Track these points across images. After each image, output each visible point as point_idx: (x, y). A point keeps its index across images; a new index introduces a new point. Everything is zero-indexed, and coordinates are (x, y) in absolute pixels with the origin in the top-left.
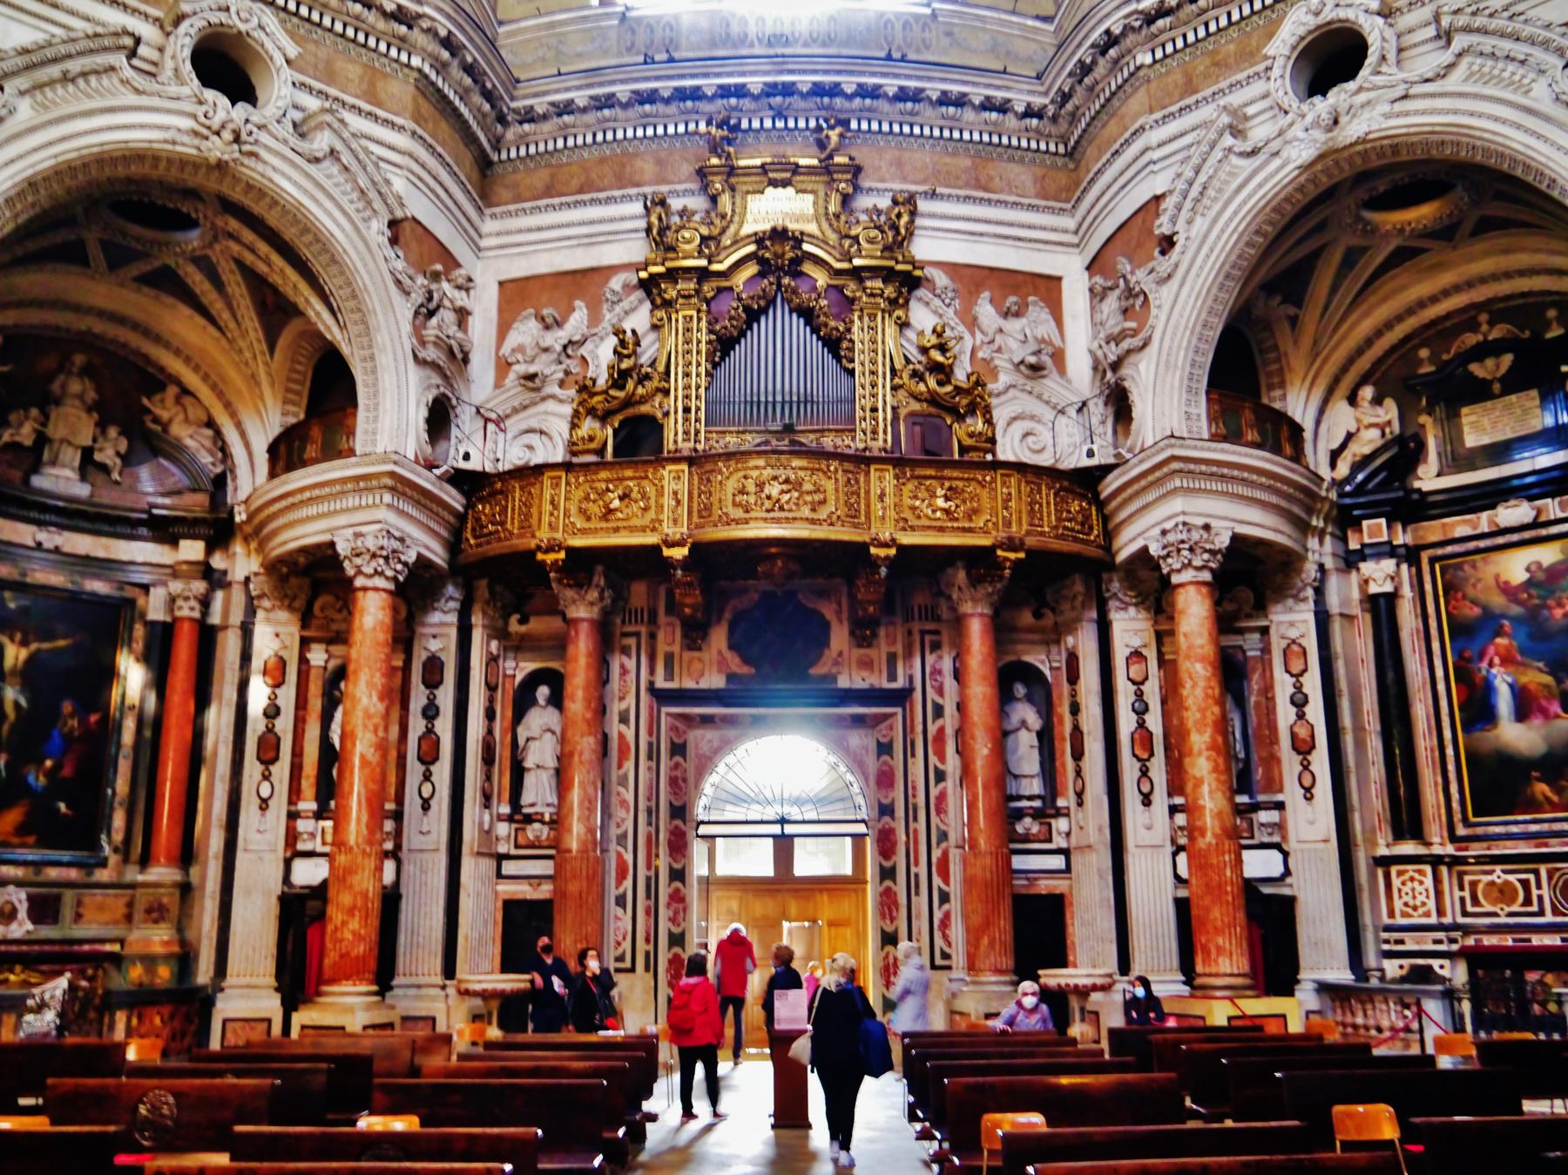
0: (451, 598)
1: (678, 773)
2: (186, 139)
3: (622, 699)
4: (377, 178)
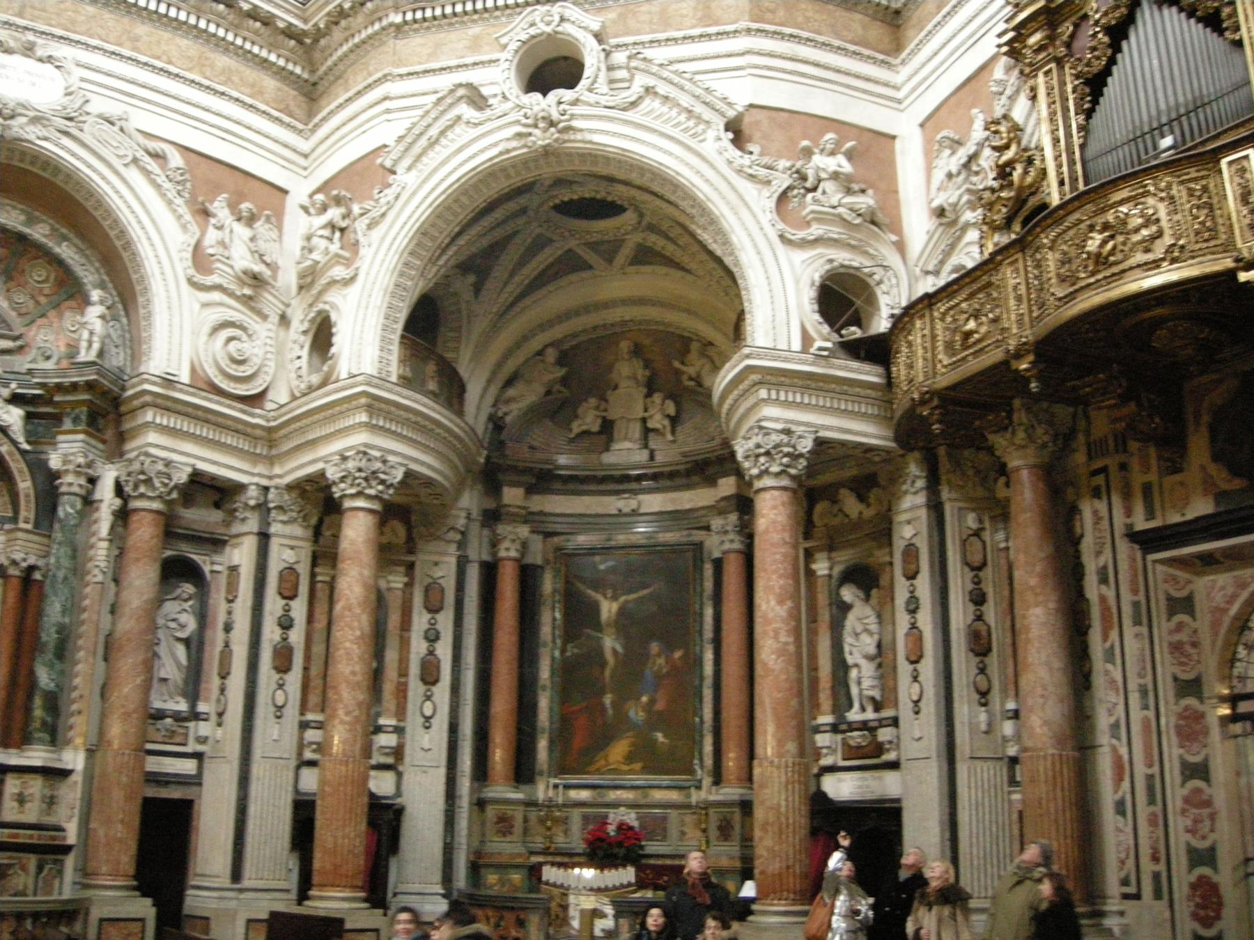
0: (918, 477)
1: (1183, 637)
2: (514, 144)
3: (1098, 553)
4: (698, 91)
